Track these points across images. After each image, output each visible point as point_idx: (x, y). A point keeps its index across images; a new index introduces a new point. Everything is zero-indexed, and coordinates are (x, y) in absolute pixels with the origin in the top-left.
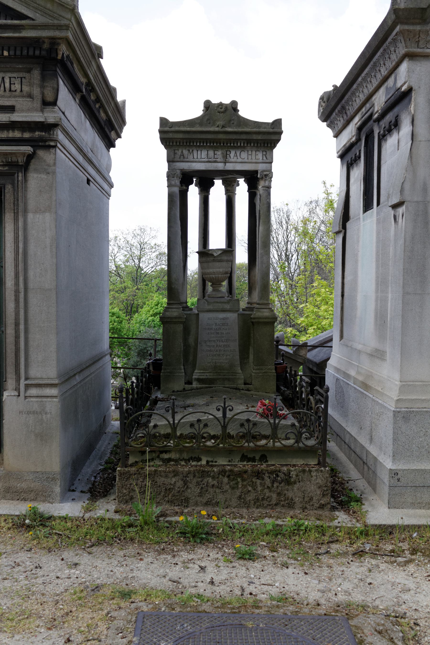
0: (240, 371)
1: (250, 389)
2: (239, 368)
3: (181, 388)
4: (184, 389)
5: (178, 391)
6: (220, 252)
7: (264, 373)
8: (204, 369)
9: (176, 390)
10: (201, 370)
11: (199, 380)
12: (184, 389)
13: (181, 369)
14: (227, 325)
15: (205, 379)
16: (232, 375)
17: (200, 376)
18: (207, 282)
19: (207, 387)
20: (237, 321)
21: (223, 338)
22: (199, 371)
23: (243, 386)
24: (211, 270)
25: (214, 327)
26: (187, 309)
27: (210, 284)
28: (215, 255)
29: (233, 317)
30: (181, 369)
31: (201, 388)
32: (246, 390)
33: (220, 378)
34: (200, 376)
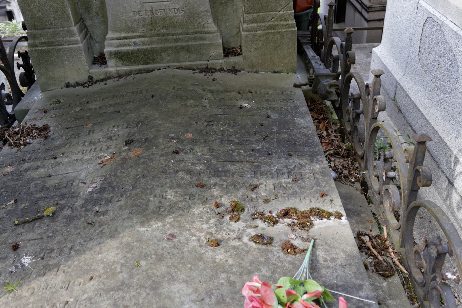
0: (213, 28)
1: (237, 68)
2: (210, 20)
3: (83, 78)
4: (90, 78)
5: (78, 84)
7: (270, 27)
8: (128, 29)
9: (72, 82)
10: (121, 31)
11: (119, 56)
12: (90, 78)
13: (71, 34)
15: (133, 52)
16: (195, 39)
17: (121, 45)
19: (140, 72)
22: (118, 35)
23: (221, 62)
31: (128, 74)
32: (229, 71)
33: (168, 48)
34: (121, 45)
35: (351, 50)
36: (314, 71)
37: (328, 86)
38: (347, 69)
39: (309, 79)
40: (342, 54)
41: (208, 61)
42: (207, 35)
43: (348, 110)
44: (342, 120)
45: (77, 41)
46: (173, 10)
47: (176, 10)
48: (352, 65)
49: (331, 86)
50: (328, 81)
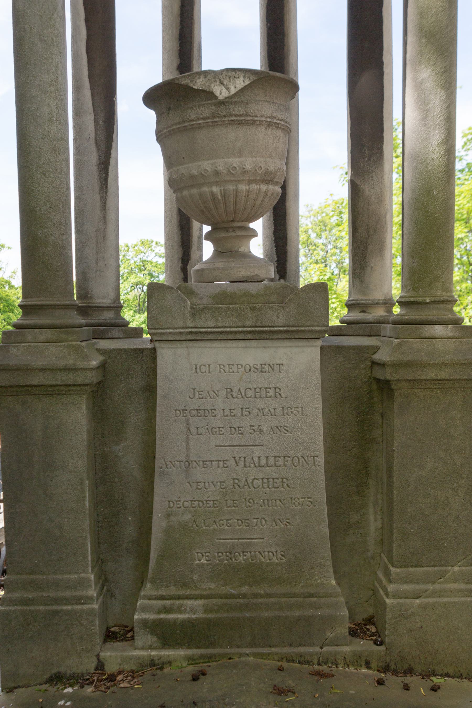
6: (240, 83)
14: (278, 395)
18: (195, 224)
20: (316, 377)
21: (258, 451)
24: (206, 165)
25: (220, 403)
26: (116, 332)
27: (207, 229)
28: (221, 92)
29: (302, 361)
30: (83, 583)
41: (321, 648)
42: (323, 600)
45: (91, 598)
46: (267, 553)
47: (270, 554)
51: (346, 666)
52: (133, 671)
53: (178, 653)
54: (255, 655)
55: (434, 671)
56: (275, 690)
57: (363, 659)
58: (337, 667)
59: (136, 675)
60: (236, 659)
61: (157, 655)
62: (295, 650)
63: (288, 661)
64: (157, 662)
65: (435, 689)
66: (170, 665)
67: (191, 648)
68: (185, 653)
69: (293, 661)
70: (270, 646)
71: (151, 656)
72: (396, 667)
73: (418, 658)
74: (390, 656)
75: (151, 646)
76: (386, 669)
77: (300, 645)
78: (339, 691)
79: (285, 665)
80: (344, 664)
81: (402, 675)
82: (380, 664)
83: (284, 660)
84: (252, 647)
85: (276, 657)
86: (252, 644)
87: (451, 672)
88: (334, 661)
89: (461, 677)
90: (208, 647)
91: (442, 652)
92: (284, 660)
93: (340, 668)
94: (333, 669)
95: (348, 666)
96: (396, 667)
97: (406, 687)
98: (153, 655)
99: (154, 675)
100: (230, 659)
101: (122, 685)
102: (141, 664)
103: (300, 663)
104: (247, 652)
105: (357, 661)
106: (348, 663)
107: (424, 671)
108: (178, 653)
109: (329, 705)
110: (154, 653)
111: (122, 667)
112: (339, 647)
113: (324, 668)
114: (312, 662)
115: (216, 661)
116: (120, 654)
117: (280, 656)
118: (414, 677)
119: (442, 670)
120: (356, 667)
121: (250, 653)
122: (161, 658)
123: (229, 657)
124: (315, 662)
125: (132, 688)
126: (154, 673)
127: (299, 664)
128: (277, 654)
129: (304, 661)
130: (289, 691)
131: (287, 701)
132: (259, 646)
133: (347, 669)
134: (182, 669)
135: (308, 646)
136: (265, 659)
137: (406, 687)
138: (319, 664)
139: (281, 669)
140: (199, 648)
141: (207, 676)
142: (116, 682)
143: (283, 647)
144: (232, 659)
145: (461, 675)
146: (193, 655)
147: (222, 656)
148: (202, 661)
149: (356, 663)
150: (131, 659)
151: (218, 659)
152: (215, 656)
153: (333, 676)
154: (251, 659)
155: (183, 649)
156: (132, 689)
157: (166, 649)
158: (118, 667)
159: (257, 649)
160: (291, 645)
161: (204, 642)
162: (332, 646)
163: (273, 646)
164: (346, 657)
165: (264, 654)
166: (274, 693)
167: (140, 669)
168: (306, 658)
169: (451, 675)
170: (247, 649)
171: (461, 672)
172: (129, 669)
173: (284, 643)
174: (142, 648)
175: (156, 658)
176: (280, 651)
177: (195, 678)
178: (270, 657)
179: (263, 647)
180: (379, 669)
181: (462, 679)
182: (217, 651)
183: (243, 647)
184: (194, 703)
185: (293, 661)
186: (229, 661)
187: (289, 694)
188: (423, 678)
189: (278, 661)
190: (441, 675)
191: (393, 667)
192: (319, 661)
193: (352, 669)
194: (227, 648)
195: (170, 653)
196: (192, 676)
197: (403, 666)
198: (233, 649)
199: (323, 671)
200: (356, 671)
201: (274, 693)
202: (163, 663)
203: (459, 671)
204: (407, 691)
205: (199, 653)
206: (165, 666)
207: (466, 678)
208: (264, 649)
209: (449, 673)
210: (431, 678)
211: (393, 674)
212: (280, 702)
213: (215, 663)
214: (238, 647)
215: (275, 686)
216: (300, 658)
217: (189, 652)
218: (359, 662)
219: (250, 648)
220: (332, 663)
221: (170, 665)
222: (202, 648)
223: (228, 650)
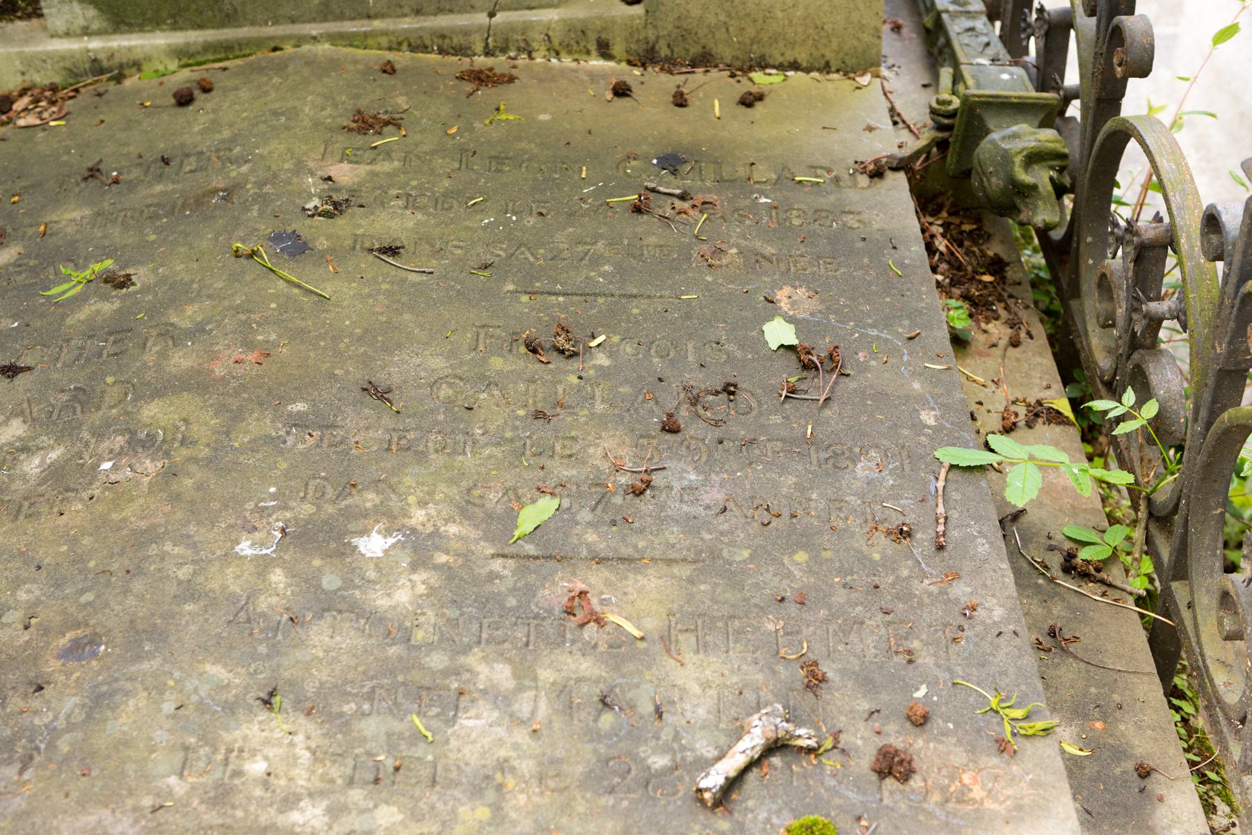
35: (1131, 11)
36: (957, 78)
37: (1018, 160)
38: (1107, 96)
39: (933, 112)
40: (1094, 20)
43: (1104, 276)
44: (1074, 304)
48: (1133, 83)
49: (1034, 158)
50: (1015, 136)
51: (553, 54)
52: (54, 88)
53: (152, 41)
54: (334, 38)
55: (763, 57)
56: (355, 121)
57: (593, 37)
58: (531, 58)
59: (61, 94)
60: (289, 49)
61: (103, 48)
62: (425, 24)
63: (413, 48)
64: (105, 64)
65: (749, 101)
66: (139, 70)
67: (181, 29)
68: (169, 41)
69: (426, 47)
70: (369, 17)
71: (88, 51)
72: (672, 52)
73: (724, 30)
74: (655, 27)
75: (87, 28)
76: (646, 58)
77: (440, 11)
78: (511, 117)
79: (402, 58)
80: (548, 50)
81: (684, 70)
82: (634, 47)
83: (405, 47)
84: (325, 20)
85: (384, 41)
86: (325, 14)
87: (803, 58)
88: (522, 45)
89: (826, 68)
90: (221, 25)
91: (780, 15)
92: (405, 47)
93: (539, 60)
94: (519, 62)
95: (558, 53)
96: (672, 52)
97: (680, 101)
98: (94, 50)
99: (100, 95)
100: (275, 49)
101: (22, 122)
102: (70, 70)
103: (441, 51)
104: (314, 33)
105: (578, 43)
106: (558, 48)
107: (738, 58)
108: (152, 41)
109: (475, 153)
110: (95, 44)
111: (27, 78)
112: (534, 11)
113: (499, 62)
114: (470, 48)
115: (244, 56)
116: (16, 49)
117: (394, 39)
118: (714, 73)
119: (782, 54)
120: (576, 56)
121: (321, 35)
122: (112, 55)
123: (273, 45)
124: (479, 47)
125: (44, 126)
126: (101, 90)
127: (440, 53)
128: (384, 33)
129: (450, 46)
130: (387, 123)
131: (375, 147)
132: (341, 17)
133: (554, 61)
134: (164, 79)
135: (459, 12)
136: (357, 47)
137: (680, 101)
138: (488, 53)
139: (389, 69)
140: (200, 27)
141: (214, 92)
142: (11, 114)
143: (399, 16)
144: (281, 49)
145: (827, 64)
146: (188, 44)
147: (258, 43)
148: (211, 57)
149: (575, 47)
150: (44, 61)
151: (248, 52)
152: (240, 45)
153: (511, 79)
154: (325, 48)
155: (164, 31)
156: (44, 130)
157: (122, 33)
158: (19, 79)
159: (339, 24)
160: (418, 12)
161: (210, 14)
162: (516, 9)
163: (377, 16)
164: (550, 33)
165: (354, 35)
166: (350, 130)
167: (72, 81)
168: (455, 40)
169: (804, 65)
170: (313, 25)
171: (827, 58)
172: (47, 82)
173: (401, 7)
174: (67, 34)
175: (102, 56)
176: (392, 27)
177: (184, 99)
178: (370, 42)
179: (352, 19)
180: (632, 58)
181: (828, 73)
182: (245, 32)
183: (304, 22)
184: (163, 159)
185: (425, 48)
186: (272, 54)
187: (390, 128)
188: (733, 76)
189: (390, 49)
190: (781, 67)
191: (664, 52)
192: (487, 44)
193: (567, 61)
194: (266, 24)
195: (133, 43)
196: (175, 95)
197: (687, 50)
198: (281, 27)
199: (491, 69)
200: (574, 64)
201: (350, 130)
202: (121, 66)
203: (823, 56)
204: (681, 110)
205: (201, 39)
206: (127, 72)
207: (838, 71)
208: (354, 23)
209: (799, 61)
210: (753, 75)
211: (662, 69)
212: (358, 149)
213: (239, 62)
214: (293, 22)
215: (359, 112)
216: (440, 42)
217: (179, 38)
218: (582, 44)
219: (322, 21)
220: (519, 49)
221: (139, 70)
222: (208, 28)
223: (271, 30)
